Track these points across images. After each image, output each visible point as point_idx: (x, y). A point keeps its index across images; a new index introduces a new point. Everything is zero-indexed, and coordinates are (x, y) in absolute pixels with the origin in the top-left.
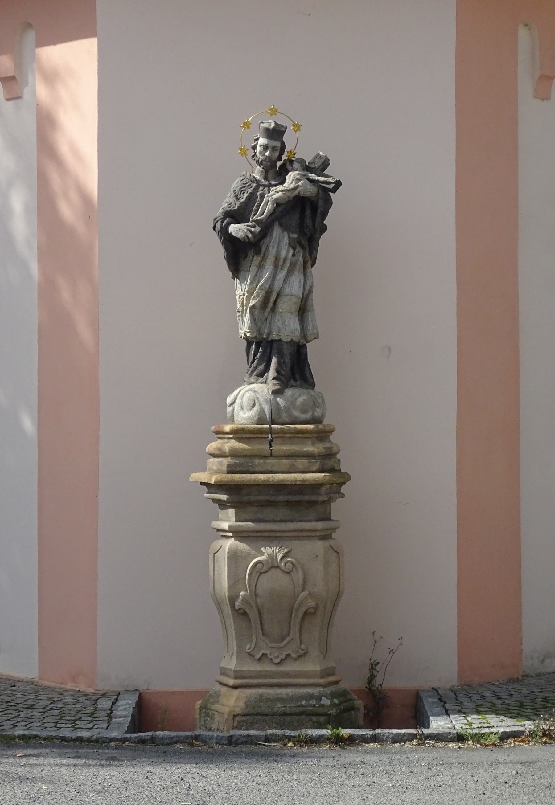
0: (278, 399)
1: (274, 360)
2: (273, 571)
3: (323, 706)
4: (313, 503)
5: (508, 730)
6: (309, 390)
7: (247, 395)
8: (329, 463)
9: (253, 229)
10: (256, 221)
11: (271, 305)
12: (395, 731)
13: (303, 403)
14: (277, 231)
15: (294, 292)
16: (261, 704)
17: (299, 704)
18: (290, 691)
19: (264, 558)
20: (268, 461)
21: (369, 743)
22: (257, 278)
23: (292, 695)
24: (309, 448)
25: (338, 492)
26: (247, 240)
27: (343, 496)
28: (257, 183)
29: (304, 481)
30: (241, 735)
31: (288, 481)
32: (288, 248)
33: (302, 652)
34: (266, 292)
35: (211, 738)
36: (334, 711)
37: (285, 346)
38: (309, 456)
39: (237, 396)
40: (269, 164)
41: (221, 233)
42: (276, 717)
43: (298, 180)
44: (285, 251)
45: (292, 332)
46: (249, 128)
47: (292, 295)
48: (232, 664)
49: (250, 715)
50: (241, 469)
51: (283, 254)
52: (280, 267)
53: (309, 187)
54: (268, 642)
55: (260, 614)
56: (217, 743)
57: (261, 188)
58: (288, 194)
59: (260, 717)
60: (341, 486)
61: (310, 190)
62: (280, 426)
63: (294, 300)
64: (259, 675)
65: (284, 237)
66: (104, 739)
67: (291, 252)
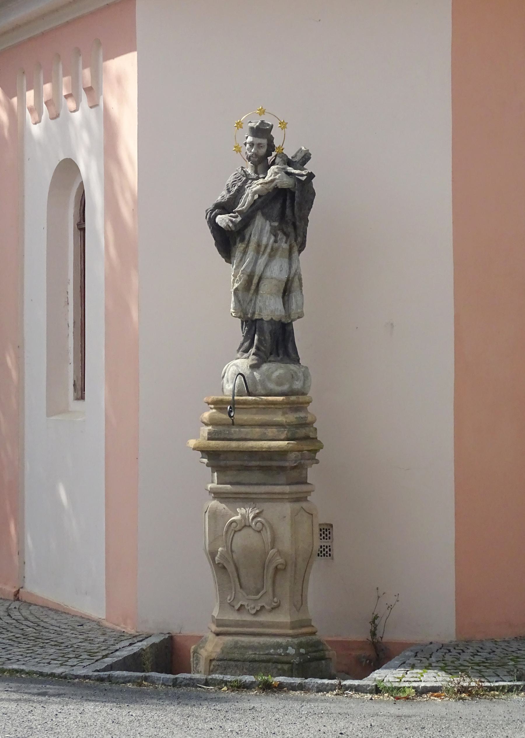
0: (255, 373)
1: (256, 337)
2: (245, 531)
3: (287, 655)
4: (282, 469)
5: (428, 685)
6: (288, 365)
7: (231, 369)
8: (302, 432)
9: (234, 219)
10: (238, 211)
11: (253, 287)
12: (320, 681)
13: (278, 377)
14: (259, 221)
15: (274, 276)
16: (236, 650)
17: (267, 652)
18: (262, 640)
19: (238, 517)
20: (242, 430)
21: (296, 691)
22: (242, 263)
23: (264, 644)
24: (279, 418)
25: (314, 459)
26: (229, 229)
27: (317, 462)
29: (270, 448)
30: (184, 678)
31: (256, 448)
32: (270, 235)
33: (275, 604)
34: (249, 276)
35: (159, 679)
36: (297, 660)
37: (266, 325)
38: (279, 425)
39: (226, 370)
40: (256, 160)
42: (246, 663)
43: (276, 173)
44: (267, 239)
45: (272, 311)
47: (272, 278)
48: (215, 613)
49: (224, 660)
50: (220, 436)
51: (264, 241)
52: (261, 253)
53: (285, 179)
54: (244, 594)
55: (237, 569)
56: (163, 684)
57: (250, 181)
58: (266, 186)
59: (233, 663)
60: (315, 454)
61: (286, 182)
62: (254, 398)
63: (274, 282)
64: (237, 624)
66: (71, 676)
67: (272, 239)
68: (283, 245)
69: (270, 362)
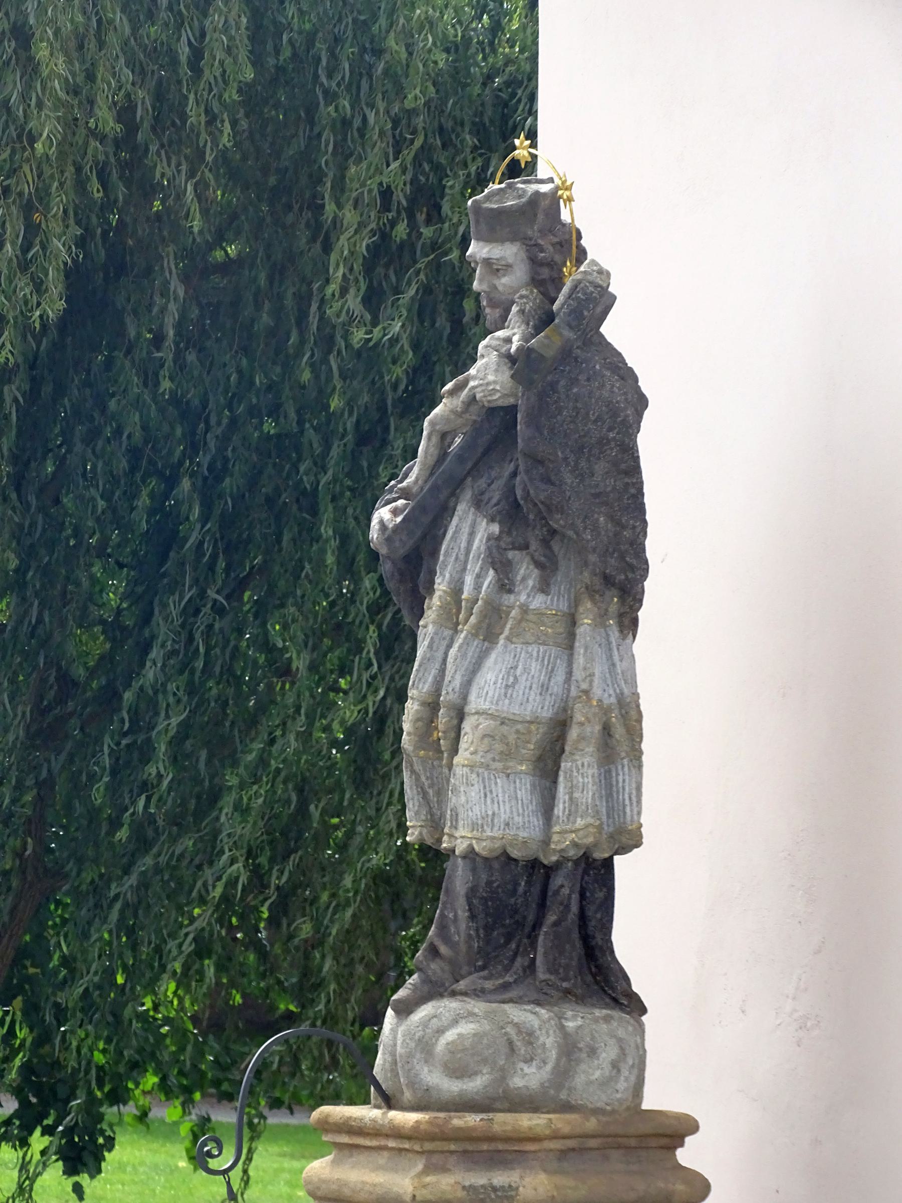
6: (506, 1007)
13: (453, 1049)
45: (474, 826)
63: (486, 724)
68: (523, 598)
69: (454, 994)
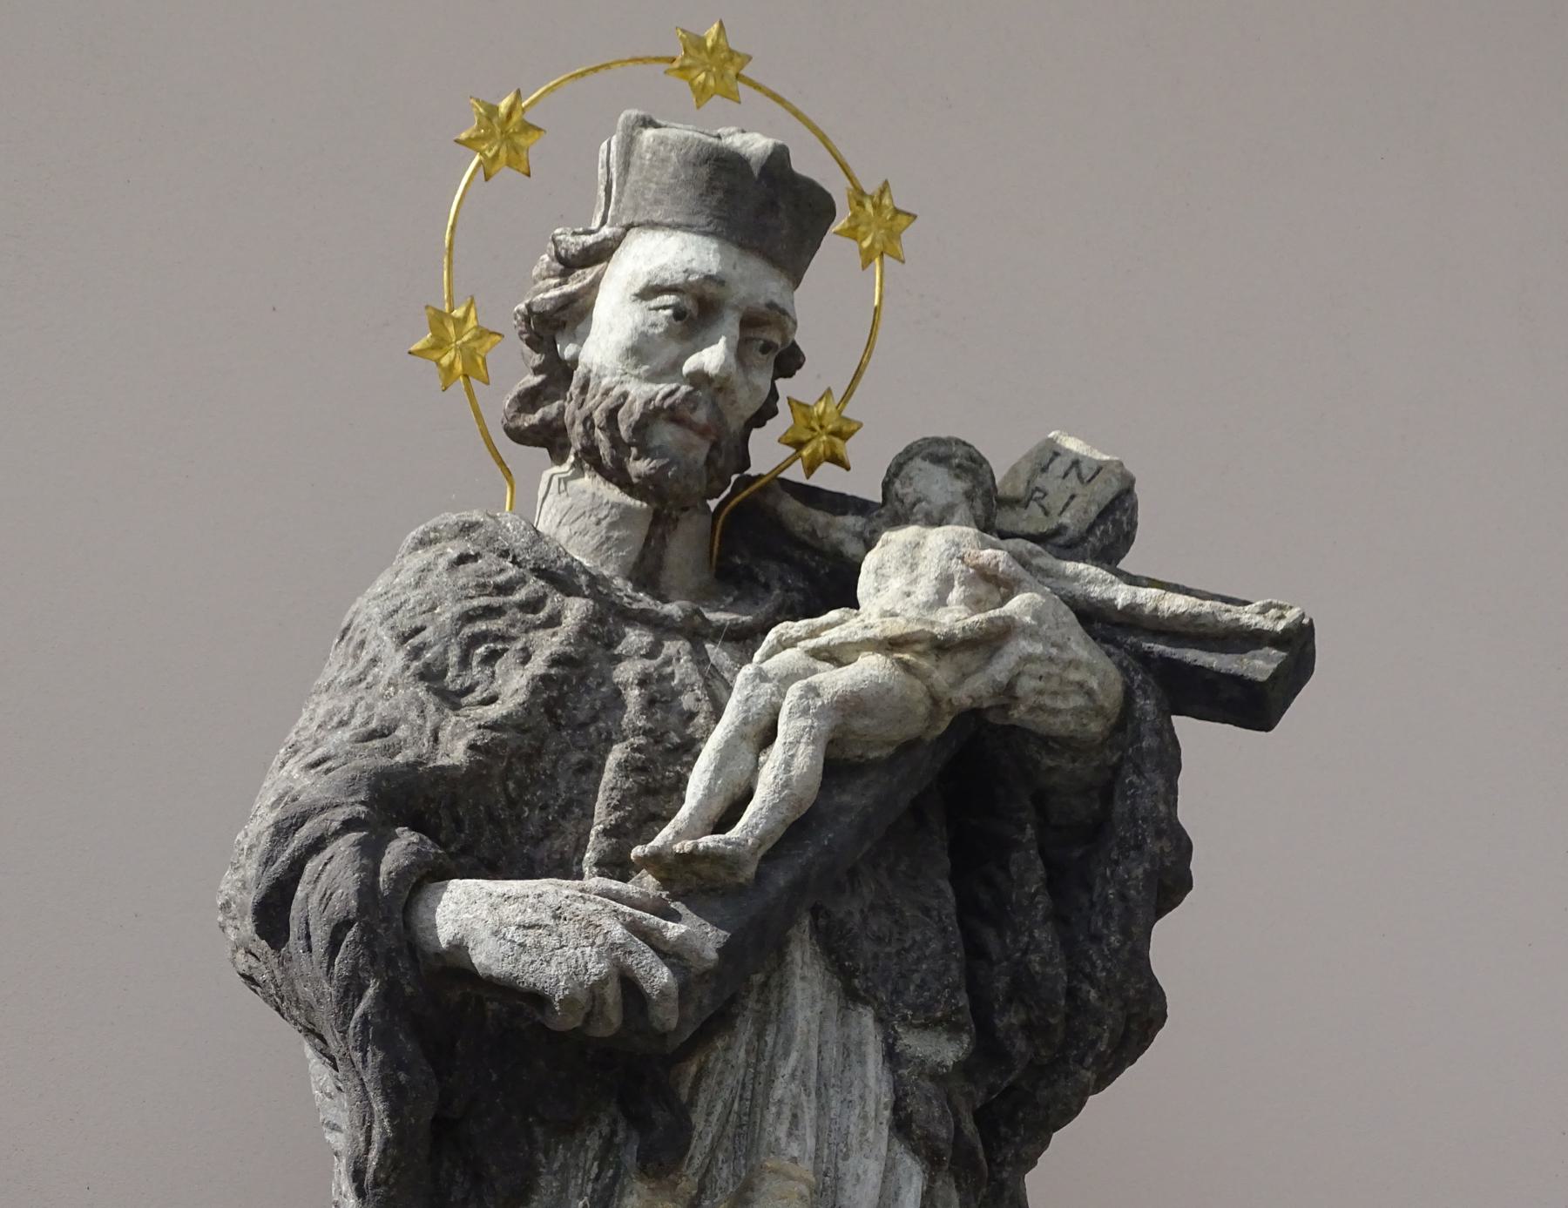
14: (807, 988)
28: (596, 596)
41: (368, 941)
46: (517, 160)
57: (636, 638)
65: (850, 1052)
